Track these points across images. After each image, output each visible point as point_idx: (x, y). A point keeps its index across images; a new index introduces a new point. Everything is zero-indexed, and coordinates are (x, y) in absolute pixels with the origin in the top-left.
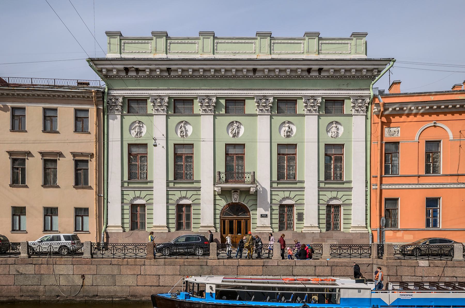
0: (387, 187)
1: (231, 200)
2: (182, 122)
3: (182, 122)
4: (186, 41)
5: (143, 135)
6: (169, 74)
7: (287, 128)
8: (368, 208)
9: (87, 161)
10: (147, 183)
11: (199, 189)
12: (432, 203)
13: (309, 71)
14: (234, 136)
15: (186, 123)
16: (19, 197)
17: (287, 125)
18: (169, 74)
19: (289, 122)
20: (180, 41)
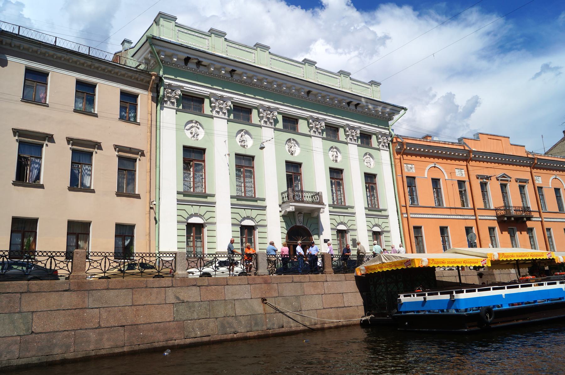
0: (413, 216)
1: (295, 223)
2: (242, 130)
3: (242, 130)
4: (244, 48)
5: (200, 137)
6: (232, 76)
7: (335, 153)
8: (402, 236)
9: (135, 160)
10: (206, 196)
11: (264, 208)
12: (443, 230)
13: (349, 104)
14: (292, 154)
15: (247, 133)
16: (26, 202)
17: (335, 150)
18: (232, 76)
19: (336, 148)
20: (237, 46)
